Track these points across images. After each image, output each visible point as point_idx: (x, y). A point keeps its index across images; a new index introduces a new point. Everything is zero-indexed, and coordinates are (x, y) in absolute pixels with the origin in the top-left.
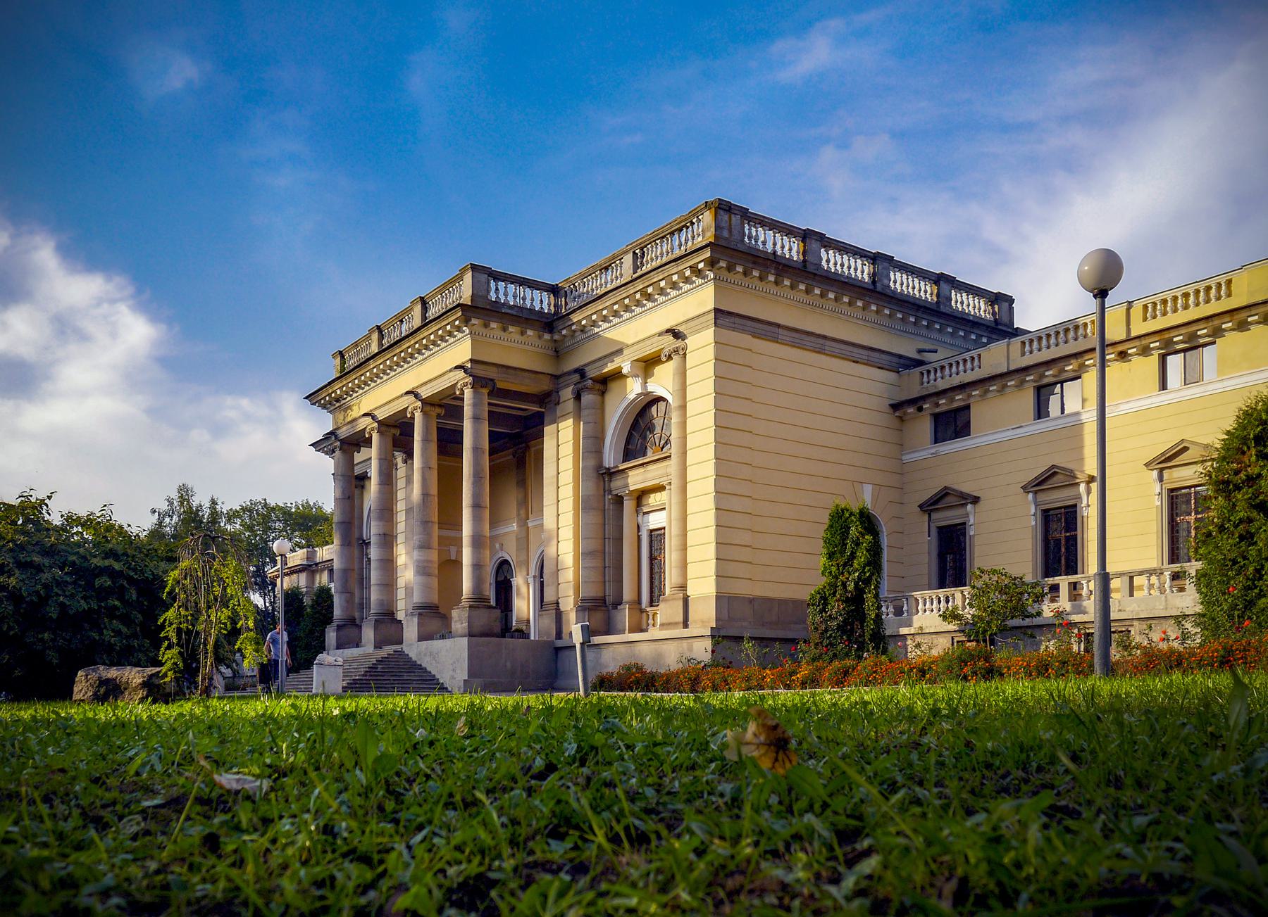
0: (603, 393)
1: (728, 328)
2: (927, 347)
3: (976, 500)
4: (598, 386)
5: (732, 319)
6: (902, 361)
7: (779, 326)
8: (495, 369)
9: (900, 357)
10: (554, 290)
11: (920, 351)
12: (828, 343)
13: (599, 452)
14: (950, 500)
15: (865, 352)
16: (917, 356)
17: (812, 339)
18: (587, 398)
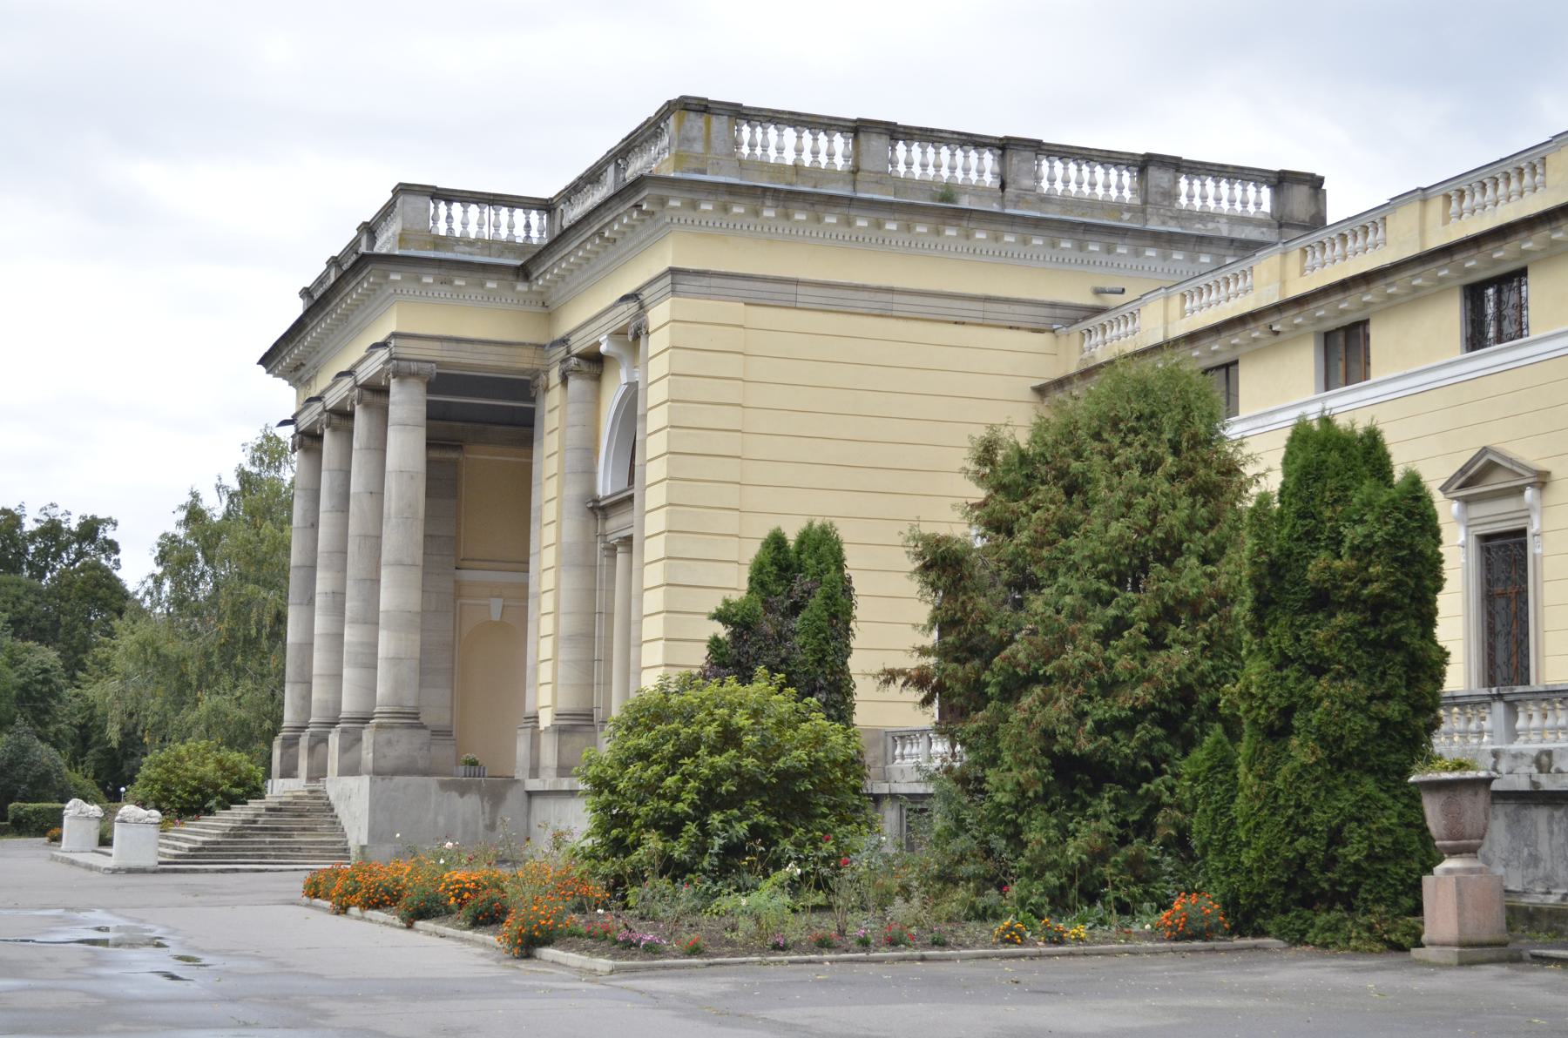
0: (598, 378)
1: (698, 295)
2: (1109, 285)
3: (1542, 480)
4: (585, 366)
5: (706, 281)
6: (1058, 312)
7: (797, 282)
8: (437, 345)
9: (1053, 305)
10: (546, 207)
11: (1098, 292)
12: (897, 298)
13: (590, 472)
14: (1497, 482)
15: (979, 306)
16: (1089, 300)
17: (865, 295)
18: (575, 384)
